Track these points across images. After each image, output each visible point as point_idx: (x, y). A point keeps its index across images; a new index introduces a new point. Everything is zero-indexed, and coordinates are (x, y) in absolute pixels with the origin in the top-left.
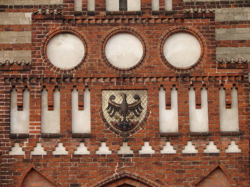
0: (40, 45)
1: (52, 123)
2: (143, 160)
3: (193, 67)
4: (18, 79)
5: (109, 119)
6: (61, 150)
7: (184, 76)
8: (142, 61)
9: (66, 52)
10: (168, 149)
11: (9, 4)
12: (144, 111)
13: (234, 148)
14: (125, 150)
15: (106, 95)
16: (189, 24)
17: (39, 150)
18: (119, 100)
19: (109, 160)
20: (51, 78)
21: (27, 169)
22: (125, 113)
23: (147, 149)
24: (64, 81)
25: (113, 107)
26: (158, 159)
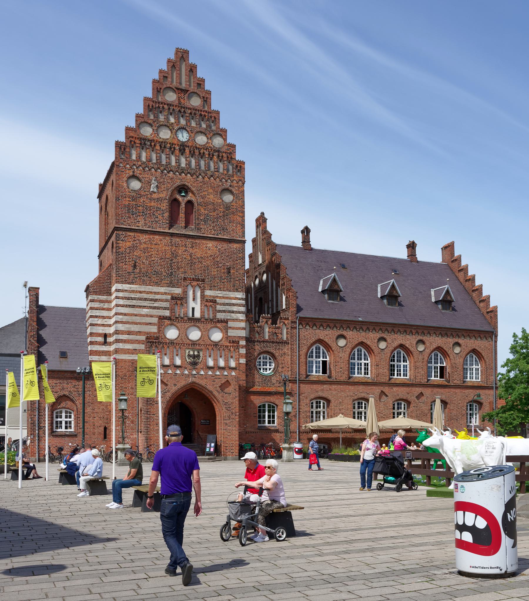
2: (200, 376)
3: (219, 342)
4: (153, 342)
5: (188, 360)
7: (216, 345)
8: (201, 338)
9: (172, 334)
10: (210, 373)
11: (136, 305)
12: (201, 358)
13: (233, 374)
16: (219, 325)
18: (192, 353)
19: (188, 376)
20: (166, 343)
23: (202, 373)
25: (189, 356)
26: (206, 376)
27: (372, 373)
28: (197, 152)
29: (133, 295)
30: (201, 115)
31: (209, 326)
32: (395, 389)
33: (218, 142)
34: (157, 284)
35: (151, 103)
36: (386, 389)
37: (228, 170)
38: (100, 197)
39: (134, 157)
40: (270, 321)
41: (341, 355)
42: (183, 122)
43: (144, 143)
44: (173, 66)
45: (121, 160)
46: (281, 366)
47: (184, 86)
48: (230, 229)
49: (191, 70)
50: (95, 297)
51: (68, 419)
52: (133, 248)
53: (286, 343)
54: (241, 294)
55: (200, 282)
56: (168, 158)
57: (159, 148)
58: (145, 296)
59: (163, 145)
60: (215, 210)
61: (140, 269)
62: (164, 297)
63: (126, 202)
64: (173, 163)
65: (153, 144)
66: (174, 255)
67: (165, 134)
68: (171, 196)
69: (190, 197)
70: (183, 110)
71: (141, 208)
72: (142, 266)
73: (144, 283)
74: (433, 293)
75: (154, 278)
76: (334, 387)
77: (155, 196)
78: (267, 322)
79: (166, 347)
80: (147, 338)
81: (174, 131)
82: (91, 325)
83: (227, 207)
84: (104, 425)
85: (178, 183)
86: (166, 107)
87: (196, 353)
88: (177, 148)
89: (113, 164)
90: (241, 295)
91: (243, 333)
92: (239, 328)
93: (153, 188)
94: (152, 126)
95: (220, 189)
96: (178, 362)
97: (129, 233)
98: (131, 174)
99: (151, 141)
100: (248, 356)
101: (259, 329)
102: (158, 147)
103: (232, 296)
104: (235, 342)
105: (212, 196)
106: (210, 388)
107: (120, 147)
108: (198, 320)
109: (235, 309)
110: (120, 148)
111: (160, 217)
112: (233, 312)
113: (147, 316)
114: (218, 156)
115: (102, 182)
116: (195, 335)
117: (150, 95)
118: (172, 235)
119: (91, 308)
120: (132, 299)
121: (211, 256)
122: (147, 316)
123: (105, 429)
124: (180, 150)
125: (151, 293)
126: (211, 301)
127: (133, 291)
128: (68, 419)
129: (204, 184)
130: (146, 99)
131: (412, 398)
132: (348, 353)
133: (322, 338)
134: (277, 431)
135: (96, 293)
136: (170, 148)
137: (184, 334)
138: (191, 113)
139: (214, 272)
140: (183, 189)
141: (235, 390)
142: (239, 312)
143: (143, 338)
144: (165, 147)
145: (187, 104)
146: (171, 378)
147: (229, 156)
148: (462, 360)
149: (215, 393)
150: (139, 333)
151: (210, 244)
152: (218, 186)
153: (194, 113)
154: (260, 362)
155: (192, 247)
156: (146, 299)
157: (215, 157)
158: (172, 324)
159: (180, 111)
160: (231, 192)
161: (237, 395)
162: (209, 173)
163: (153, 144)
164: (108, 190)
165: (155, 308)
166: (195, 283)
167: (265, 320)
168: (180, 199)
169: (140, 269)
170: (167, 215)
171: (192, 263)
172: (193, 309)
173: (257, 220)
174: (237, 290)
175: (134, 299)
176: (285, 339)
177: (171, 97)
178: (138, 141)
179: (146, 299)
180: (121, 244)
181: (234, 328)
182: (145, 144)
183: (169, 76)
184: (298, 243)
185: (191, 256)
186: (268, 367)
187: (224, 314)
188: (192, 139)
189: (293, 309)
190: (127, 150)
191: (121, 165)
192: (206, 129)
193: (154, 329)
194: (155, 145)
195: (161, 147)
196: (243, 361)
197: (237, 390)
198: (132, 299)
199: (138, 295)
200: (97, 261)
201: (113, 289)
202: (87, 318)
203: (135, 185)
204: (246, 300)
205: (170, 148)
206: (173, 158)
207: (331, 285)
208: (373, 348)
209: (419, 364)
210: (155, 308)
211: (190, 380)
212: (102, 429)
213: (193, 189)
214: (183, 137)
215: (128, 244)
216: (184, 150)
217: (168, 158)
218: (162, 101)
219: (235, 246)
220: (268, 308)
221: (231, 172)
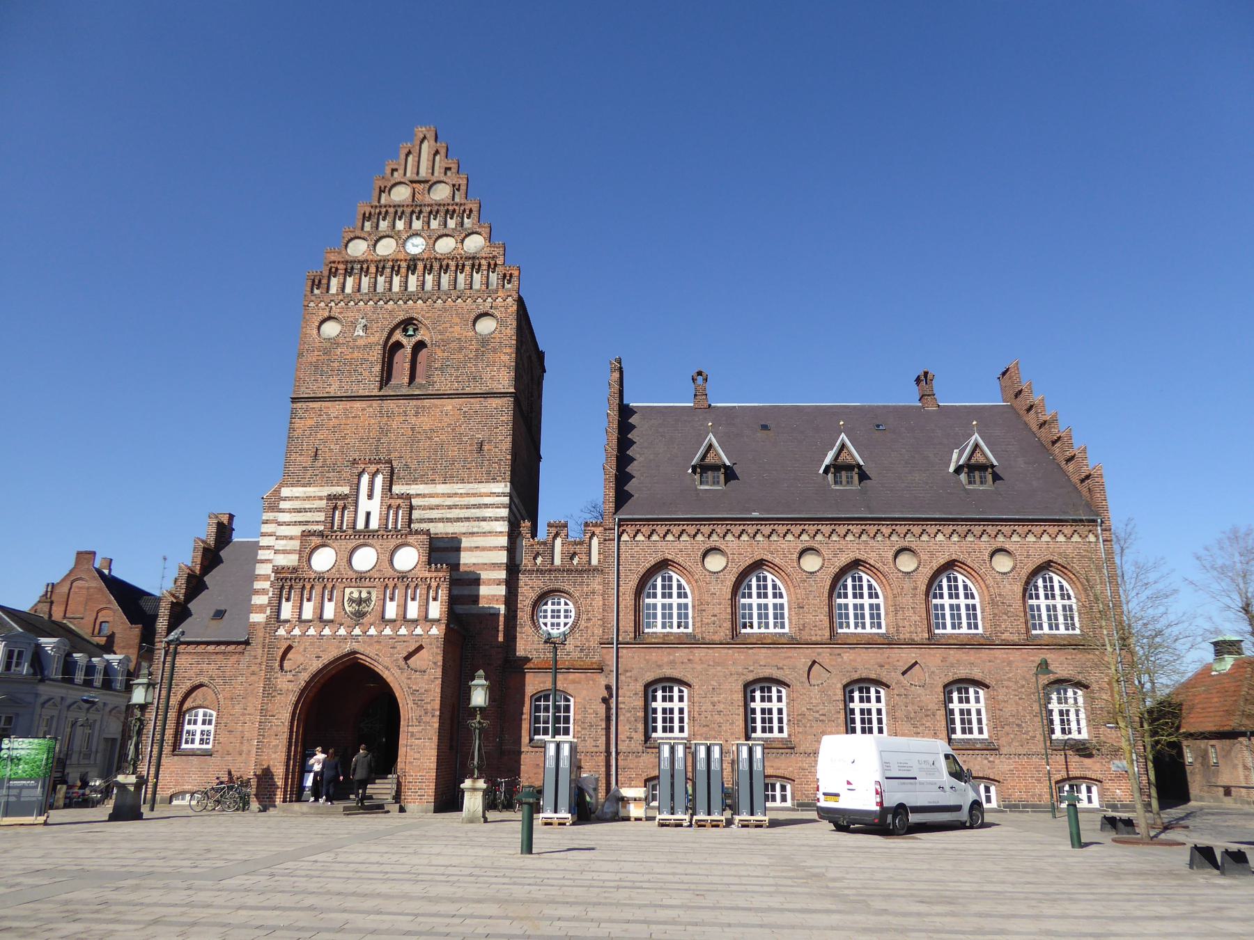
0: (307, 554)
2: (367, 639)
5: (347, 609)
9: (324, 560)
10: (388, 631)
15: (348, 591)
16: (411, 539)
17: (297, 632)
18: (356, 595)
22: (359, 604)
23: (372, 631)
25: (351, 600)
26: (378, 639)
27: (790, 623)
28: (436, 266)
29: (307, 505)
31: (392, 543)
32: (847, 655)
36: (824, 655)
39: (333, 290)
43: (351, 267)
46: (585, 617)
53: (596, 569)
54: (503, 485)
60: (461, 349)
61: (325, 460)
63: (312, 358)
65: (365, 266)
66: (384, 431)
67: (386, 248)
71: (336, 364)
76: (699, 653)
77: (360, 342)
83: (484, 341)
87: (364, 595)
88: (404, 264)
90: (503, 487)
97: (312, 405)
98: (326, 314)
102: (373, 269)
103: (483, 490)
105: (457, 328)
109: (488, 513)
111: (366, 373)
112: (484, 519)
114: (473, 265)
124: (408, 268)
127: (308, 498)
129: (446, 310)
133: (670, 557)
139: (453, 451)
140: (407, 324)
141: (435, 663)
142: (497, 519)
145: (427, 200)
146: (312, 644)
147: (492, 262)
148: (1018, 589)
151: (449, 405)
154: (566, 617)
157: (467, 268)
158: (324, 546)
163: (365, 266)
168: (404, 341)
169: (325, 460)
170: (378, 368)
171: (414, 440)
172: (368, 514)
174: (494, 480)
175: (310, 510)
177: (401, 194)
185: (413, 429)
186: (562, 620)
187: (467, 524)
195: (377, 268)
197: (440, 663)
203: (331, 329)
205: (393, 268)
208: (789, 570)
209: (907, 600)
211: (347, 648)
214: (416, 246)
215: (310, 422)
216: (415, 266)
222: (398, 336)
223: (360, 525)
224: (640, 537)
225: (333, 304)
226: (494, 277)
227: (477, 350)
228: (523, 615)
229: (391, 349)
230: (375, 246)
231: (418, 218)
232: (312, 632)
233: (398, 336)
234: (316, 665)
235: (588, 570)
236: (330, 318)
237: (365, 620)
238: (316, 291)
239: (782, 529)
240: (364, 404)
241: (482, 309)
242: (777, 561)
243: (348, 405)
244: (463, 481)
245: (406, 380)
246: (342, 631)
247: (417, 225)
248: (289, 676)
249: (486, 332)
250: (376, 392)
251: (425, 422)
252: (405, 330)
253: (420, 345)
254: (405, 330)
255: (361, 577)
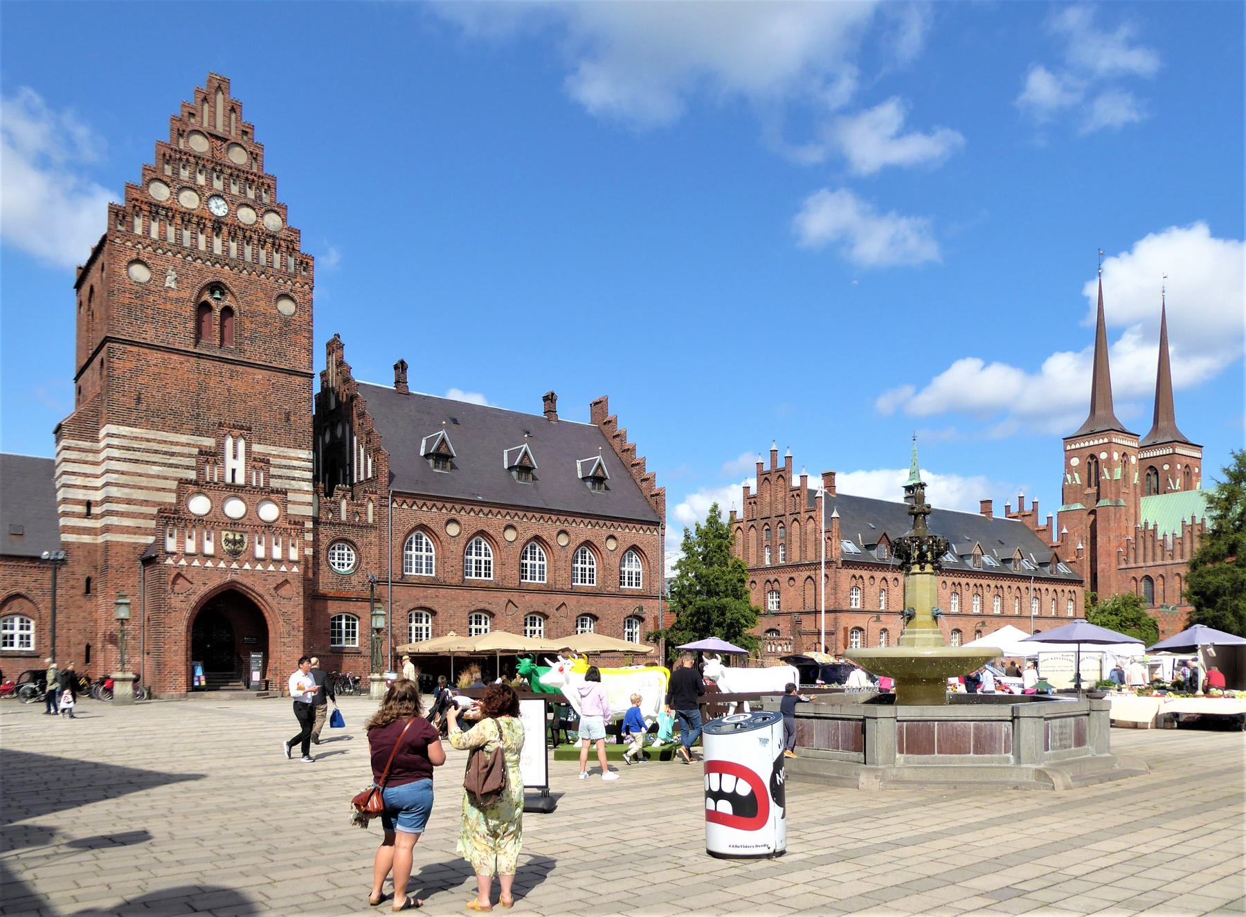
1: (191, 546)
6: (196, 563)
10: (259, 567)
13: (295, 569)
14: (235, 566)
17: (183, 562)
19: (225, 571)
21: (175, 572)
23: (247, 566)
24: (200, 521)
26: (253, 573)
28: (240, 233)
30: (247, 179)
33: (272, 222)
34: (175, 430)
35: (168, 152)
37: (287, 266)
38: (78, 286)
39: (138, 231)
40: (349, 496)
41: (453, 547)
42: (218, 185)
43: (155, 210)
44: (205, 100)
45: (118, 234)
47: (220, 129)
48: (290, 354)
49: (233, 110)
50: (72, 443)
51: (25, 632)
52: (136, 371)
55: (244, 430)
56: (194, 238)
57: (179, 222)
58: (155, 446)
59: (186, 218)
60: (266, 324)
62: (186, 450)
64: (202, 247)
65: (170, 214)
67: (189, 201)
68: (199, 296)
69: (228, 301)
70: (218, 168)
71: (149, 311)
72: (151, 400)
73: (154, 426)
74: (579, 466)
75: (171, 421)
77: (171, 294)
78: (344, 496)
79: (190, 526)
80: (160, 511)
81: (204, 199)
82: (64, 486)
83: (287, 321)
84: (85, 642)
85: (210, 279)
86: (192, 160)
88: (209, 224)
89: (104, 239)
90: (307, 454)
91: (309, 511)
92: (303, 501)
93: (170, 282)
94: (168, 185)
95: (275, 294)
96: (209, 548)
97: (129, 348)
98: (134, 256)
99: (168, 209)
100: (315, 544)
101: (332, 506)
104: (298, 523)
105: (262, 303)
106: (259, 589)
107: (117, 214)
108: (240, 488)
109: (297, 474)
110: (117, 215)
111: (180, 327)
112: (294, 479)
113: (158, 477)
114: (274, 244)
115: (83, 263)
116: (235, 508)
117: (166, 139)
118: (199, 356)
119: (65, 460)
120: (134, 449)
121: (260, 393)
122: (158, 477)
123: (88, 647)
124: (214, 229)
125: (165, 442)
126: (262, 461)
128: (25, 632)
130: (160, 144)
131: (550, 611)
132: (462, 545)
134: (358, 653)
135: (73, 437)
136: (198, 224)
137: (218, 507)
138: (231, 175)
139: (265, 417)
140: (216, 287)
142: (304, 480)
143: (154, 511)
144: (189, 221)
146: (198, 573)
149: (267, 597)
150: (145, 503)
151: (259, 375)
152: (273, 289)
153: (236, 174)
155: (231, 377)
156: (156, 452)
159: (214, 169)
160: (292, 299)
161: (301, 602)
162: (259, 269)
163: (170, 214)
164: (94, 277)
165: (171, 466)
166: (236, 432)
167: (341, 493)
168: (213, 303)
171: (230, 402)
173: (328, 345)
174: (300, 447)
176: (370, 520)
177: (199, 145)
178: (145, 207)
179: (156, 452)
180: (117, 364)
181: (295, 503)
182: (157, 213)
183: (198, 114)
184: (387, 382)
185: (229, 390)
188: (232, 213)
189: (384, 480)
190: (128, 219)
191: (117, 240)
192: (254, 201)
193: (171, 498)
194: (173, 217)
196: (309, 552)
198: (134, 449)
199: (144, 445)
200: (72, 387)
201: (103, 432)
202: (57, 474)
204: (316, 461)
205: (198, 224)
206: (202, 239)
207: (438, 448)
210: (171, 466)
212: (83, 648)
213: (233, 290)
214: (219, 208)
215: (128, 365)
216: (220, 229)
217: (194, 238)
218: (186, 150)
219: (299, 380)
220: (345, 475)
221: (292, 270)
222: (206, 297)
223: (229, 480)
224: (405, 506)
225: (140, 246)
226: (291, 261)
227: (281, 328)
228: (322, 558)
229: (204, 308)
230: (177, 194)
231: (218, 178)
232: (196, 563)
233: (206, 297)
234: (202, 590)
235: (365, 527)
236: (137, 261)
237: (240, 558)
238: (120, 228)
239: (495, 511)
240: (182, 358)
241: (283, 290)
242: (491, 532)
243: (166, 356)
244: (274, 444)
245: (217, 342)
246: (222, 565)
247: (218, 185)
248: (182, 597)
249: (286, 313)
250: (191, 349)
251: (239, 386)
252: (212, 293)
253: (227, 311)
254: (212, 293)
255: (234, 523)
